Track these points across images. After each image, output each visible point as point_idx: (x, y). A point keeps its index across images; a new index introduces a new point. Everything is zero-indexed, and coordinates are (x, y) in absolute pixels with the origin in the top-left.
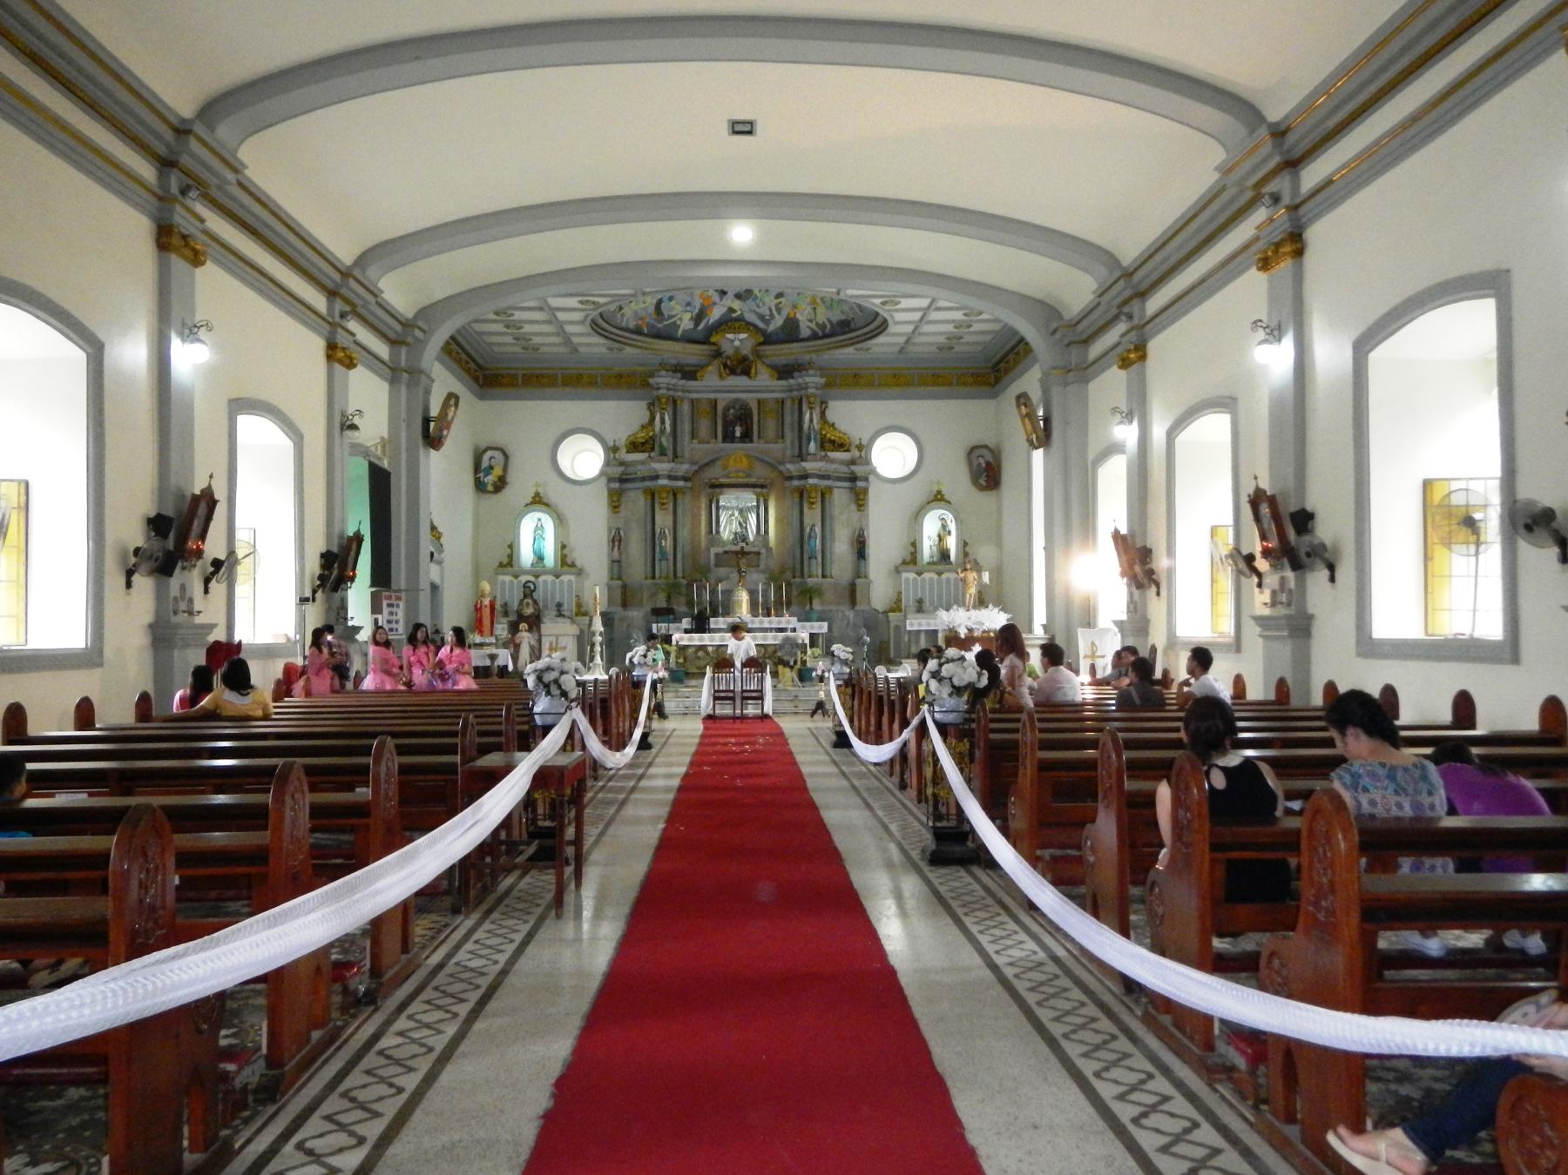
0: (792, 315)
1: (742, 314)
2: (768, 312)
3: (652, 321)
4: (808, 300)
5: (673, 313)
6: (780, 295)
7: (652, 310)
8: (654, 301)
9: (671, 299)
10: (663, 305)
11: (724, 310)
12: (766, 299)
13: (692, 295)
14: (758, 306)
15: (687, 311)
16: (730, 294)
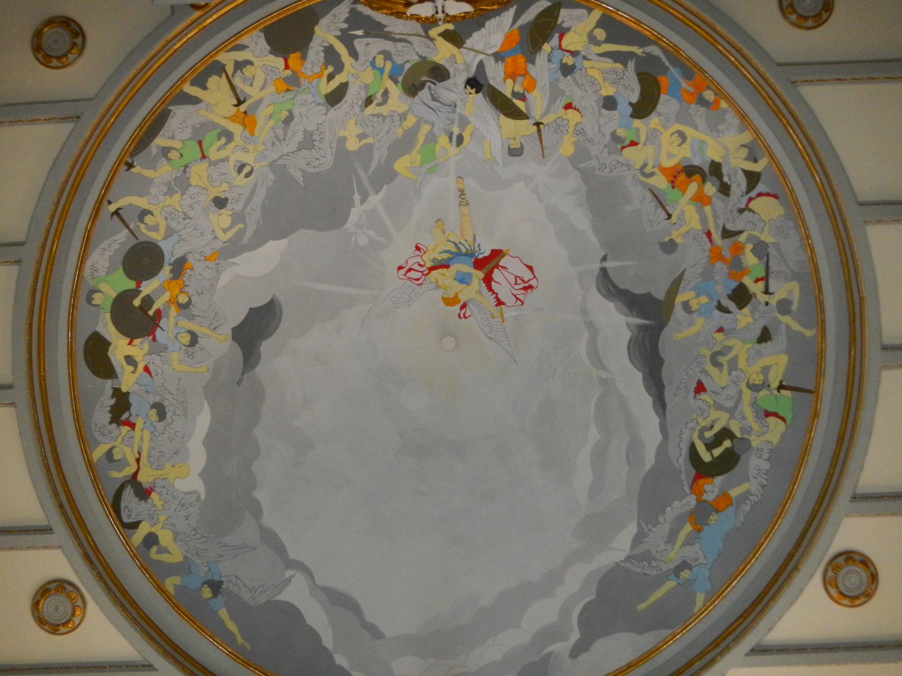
0: (293, 58)
1: (426, 30)
2: (359, 45)
3: (672, 69)
4: (262, 115)
5: (608, 64)
6: (335, 97)
7: (667, 104)
8: (654, 121)
9: (610, 103)
10: (635, 97)
11: (476, 40)
12: (368, 76)
13: (555, 92)
14: (387, 55)
15: (574, 54)
16: (459, 79)
